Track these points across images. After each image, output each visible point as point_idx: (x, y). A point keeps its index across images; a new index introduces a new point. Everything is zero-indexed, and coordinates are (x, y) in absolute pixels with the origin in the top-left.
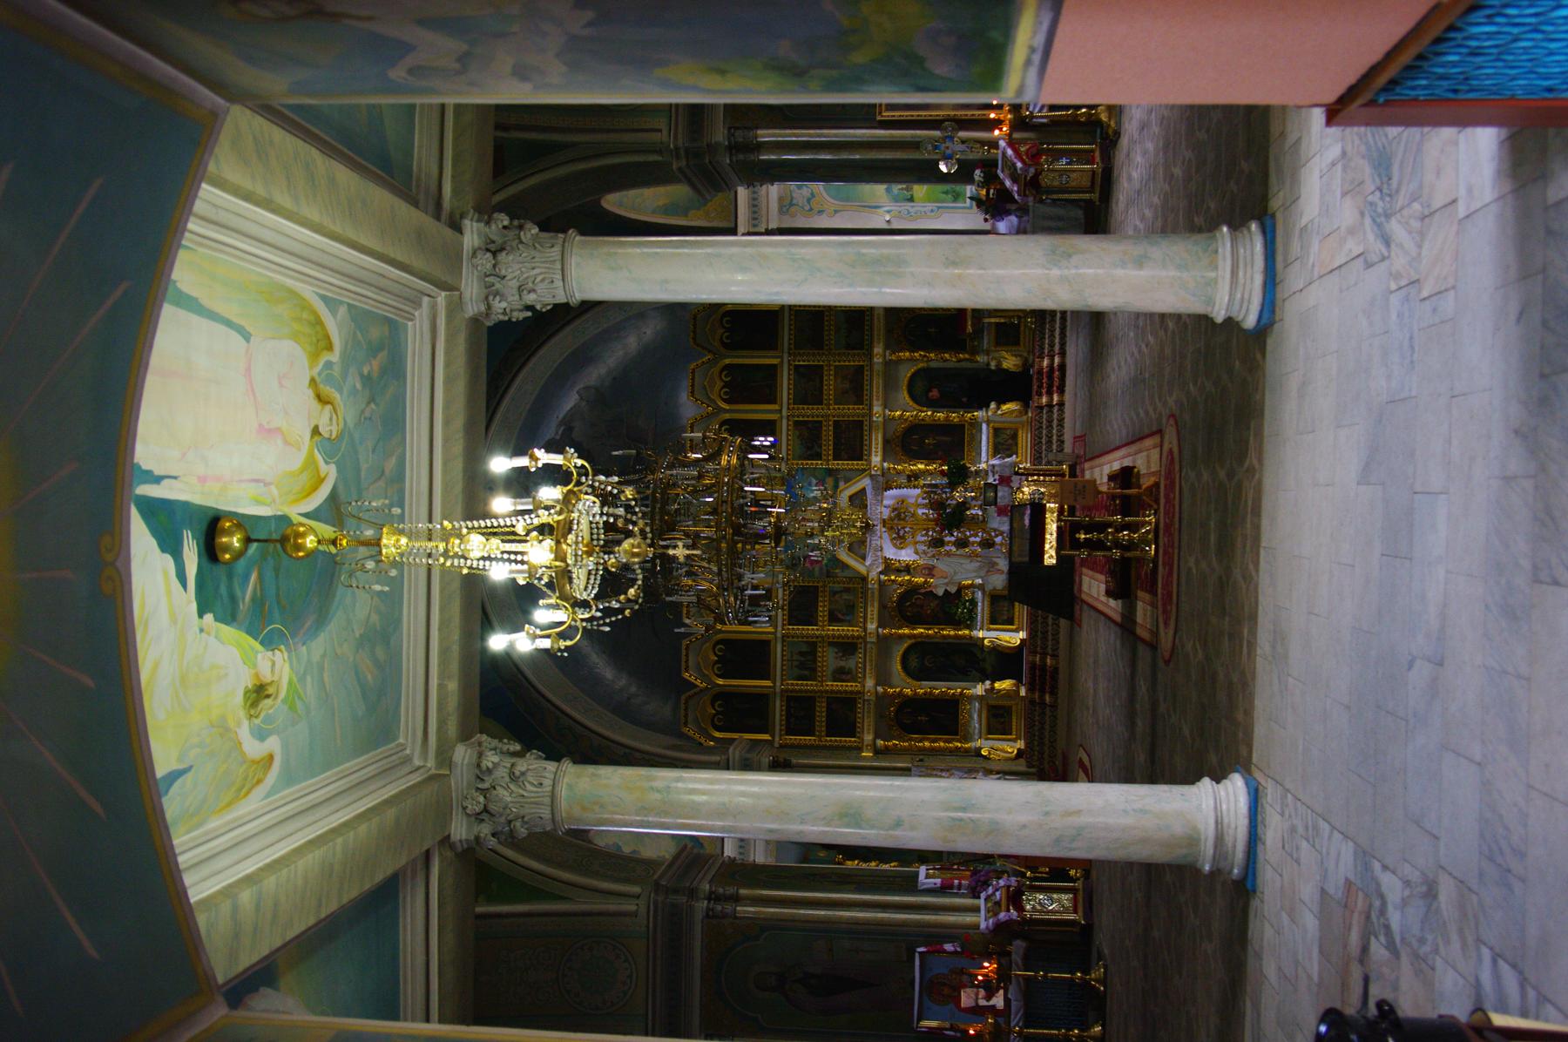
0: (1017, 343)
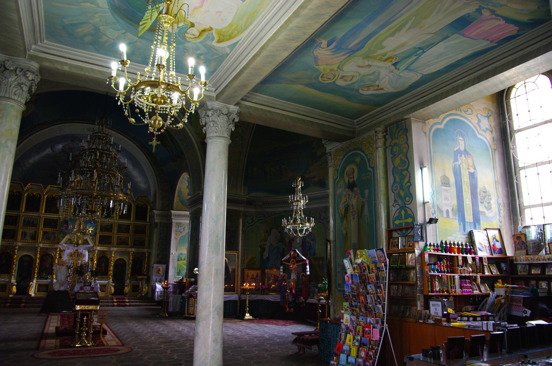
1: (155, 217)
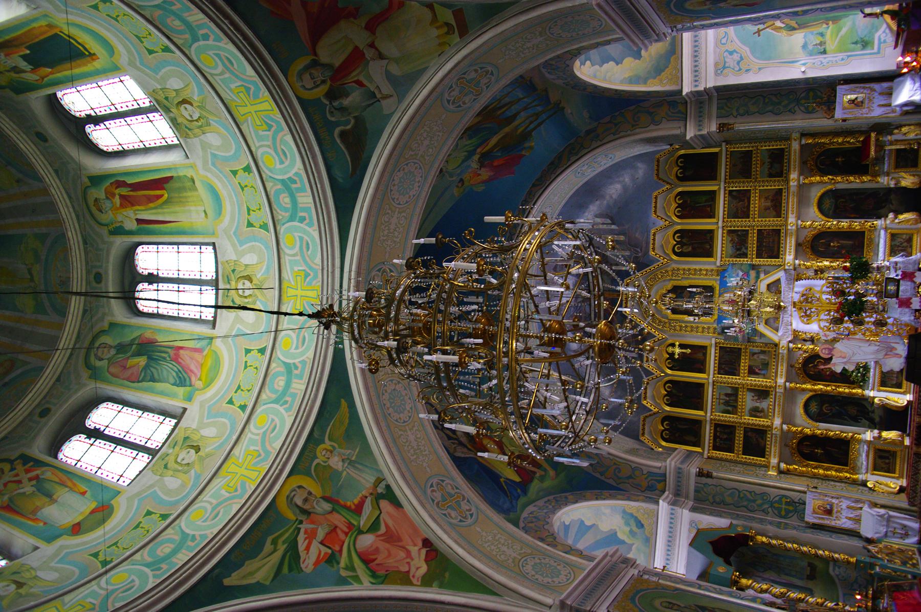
1: (704, 132)
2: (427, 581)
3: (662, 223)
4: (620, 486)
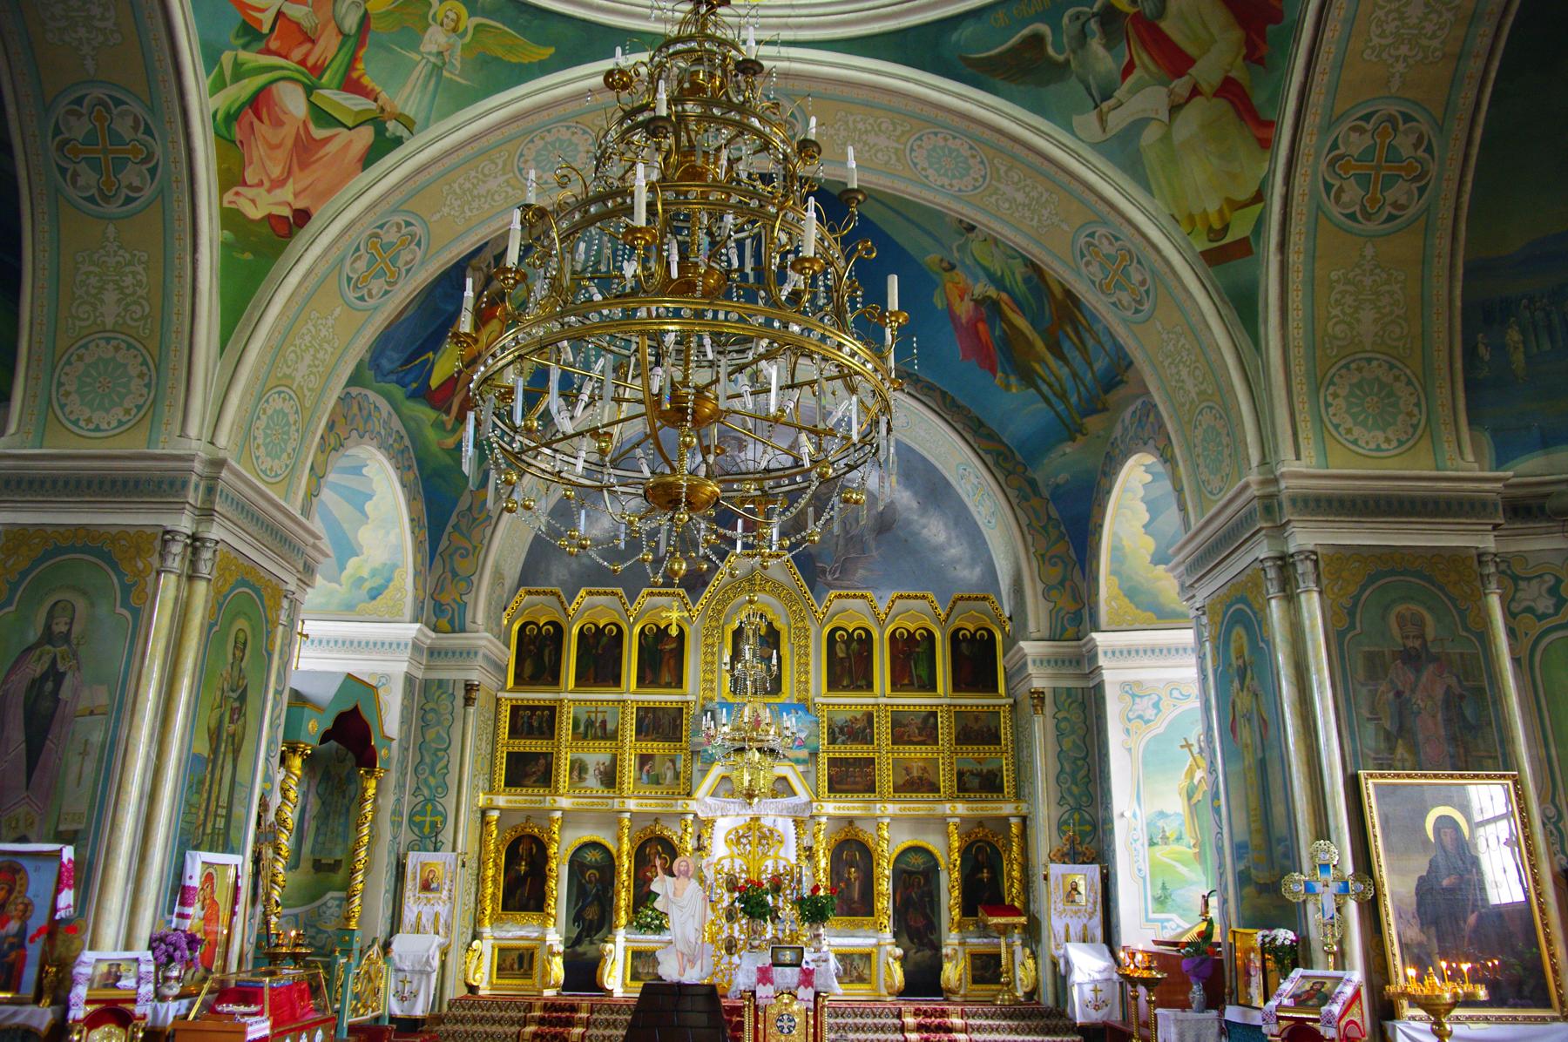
0: (975, 981)
1: (1031, 669)
2: (231, 219)
3: (882, 608)
4: (437, 556)
